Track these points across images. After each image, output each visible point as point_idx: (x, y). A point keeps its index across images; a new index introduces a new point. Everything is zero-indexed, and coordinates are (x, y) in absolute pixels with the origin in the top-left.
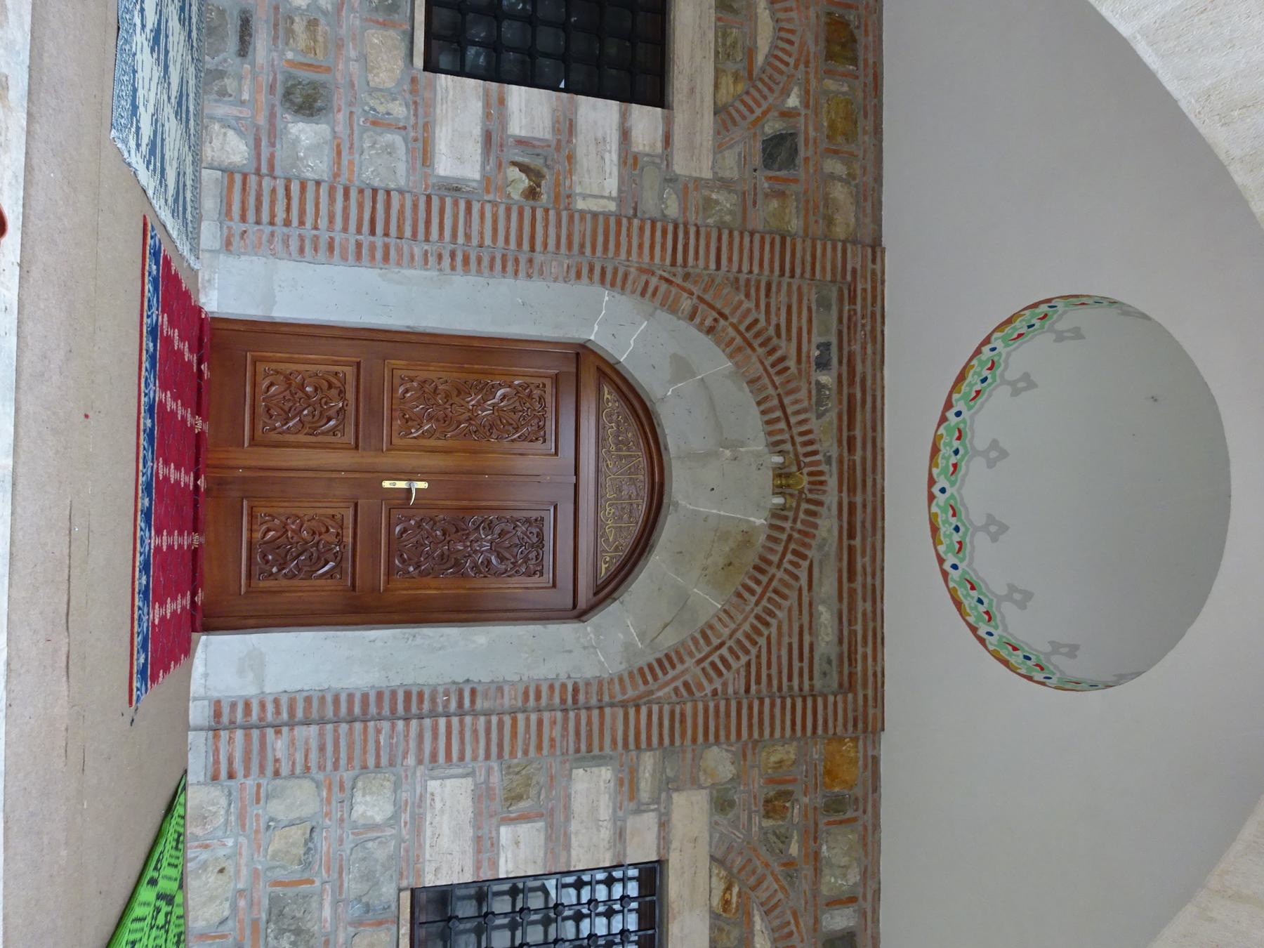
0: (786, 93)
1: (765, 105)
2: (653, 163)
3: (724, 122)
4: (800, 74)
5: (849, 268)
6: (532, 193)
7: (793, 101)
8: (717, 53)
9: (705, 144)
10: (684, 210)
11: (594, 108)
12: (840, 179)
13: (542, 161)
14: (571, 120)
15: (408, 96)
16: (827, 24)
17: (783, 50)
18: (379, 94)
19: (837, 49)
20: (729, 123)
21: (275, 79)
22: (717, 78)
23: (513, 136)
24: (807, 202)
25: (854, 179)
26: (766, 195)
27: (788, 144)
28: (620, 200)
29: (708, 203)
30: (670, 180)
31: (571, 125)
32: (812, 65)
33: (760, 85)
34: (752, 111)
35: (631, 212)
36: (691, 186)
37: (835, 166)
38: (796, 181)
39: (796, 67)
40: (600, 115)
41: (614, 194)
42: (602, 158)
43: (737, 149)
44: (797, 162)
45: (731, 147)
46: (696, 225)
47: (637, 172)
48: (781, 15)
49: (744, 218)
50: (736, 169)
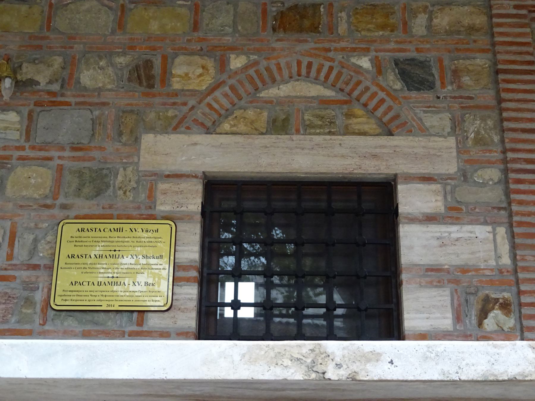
0: (358, 70)
1: (374, 89)
2: (452, 192)
3: (397, 127)
4: (339, 57)
5: (515, 12)
6: (505, 306)
7: (365, 63)
8: (330, 133)
9: (423, 144)
10: (490, 163)
11: (411, 248)
12: (430, 19)
13: (472, 298)
14: (427, 270)
16: (285, 30)
17: (319, 71)
19: (307, 23)
20: (397, 122)
22: (354, 133)
23: (454, 325)
24: (458, 50)
25: (427, 7)
26: (459, 87)
27: (408, 68)
28: (495, 224)
29: (479, 141)
30: (465, 176)
31: (432, 270)
32: (327, 45)
33: (356, 93)
34: (382, 101)
35: (503, 212)
36: (466, 157)
37: (419, 25)
38: (440, 61)
39: (332, 60)
40: (416, 244)
41: (489, 228)
42: (457, 240)
43: (422, 115)
44: (422, 59)
45: (421, 120)
46: (504, 152)
47: (464, 208)
48: (286, 73)
49: (487, 107)
50: (441, 115)
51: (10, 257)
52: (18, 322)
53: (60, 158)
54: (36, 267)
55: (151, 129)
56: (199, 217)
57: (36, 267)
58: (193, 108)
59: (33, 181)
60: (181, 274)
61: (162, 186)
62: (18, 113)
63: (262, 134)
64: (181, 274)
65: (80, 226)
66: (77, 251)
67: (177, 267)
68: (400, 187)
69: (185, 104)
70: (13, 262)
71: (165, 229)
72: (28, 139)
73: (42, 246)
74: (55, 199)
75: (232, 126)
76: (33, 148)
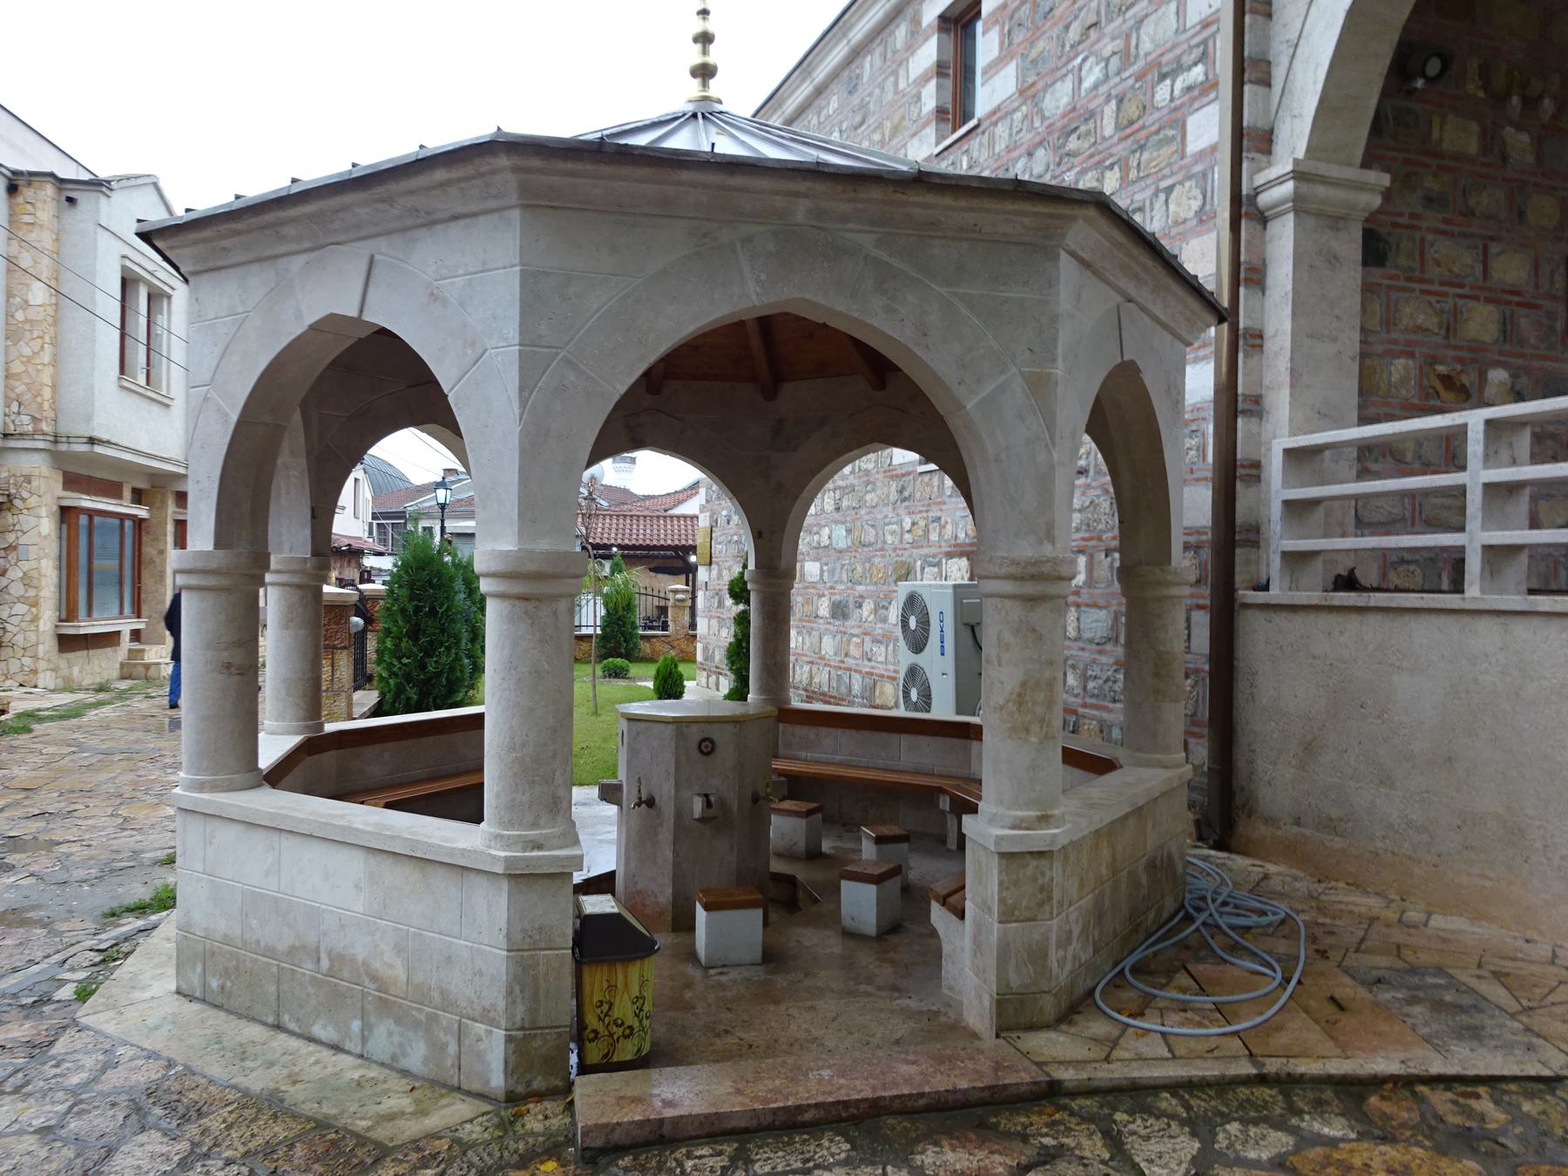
51: (1537, 286)
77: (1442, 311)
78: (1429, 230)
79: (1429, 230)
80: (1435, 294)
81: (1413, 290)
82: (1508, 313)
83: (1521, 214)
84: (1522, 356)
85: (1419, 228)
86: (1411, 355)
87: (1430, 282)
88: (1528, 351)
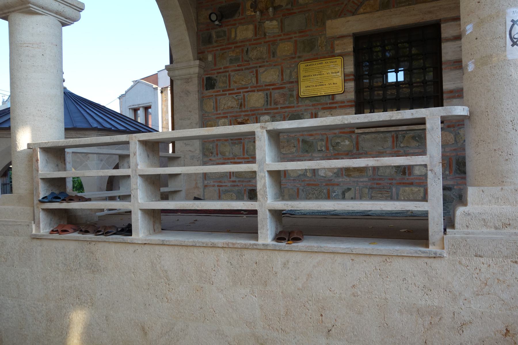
8: (409, 5)
14: (455, 62)
15: (456, 128)
18: (457, 139)
21: (459, 177)
51: (282, 80)
52: (289, 103)
53: (295, 37)
54: (292, 82)
55: (329, 18)
56: (352, 53)
57: (292, 82)
58: (346, 4)
59: (286, 48)
60: (347, 78)
61: (336, 42)
62: (277, 20)
63: (378, 11)
64: (347, 78)
65: (306, 64)
66: (307, 74)
67: (345, 75)
68: (442, 25)
69: (343, 3)
70: (284, 81)
71: (339, 61)
72: (282, 31)
73: (294, 74)
74: (295, 53)
75: (364, 10)
76: (284, 35)
77: (238, 99)
78: (232, 71)
79: (232, 71)
80: (235, 93)
81: (226, 94)
82: (269, 94)
83: (274, 54)
84: (277, 108)
85: (228, 71)
86: (226, 117)
87: (233, 90)
88: (279, 106)
